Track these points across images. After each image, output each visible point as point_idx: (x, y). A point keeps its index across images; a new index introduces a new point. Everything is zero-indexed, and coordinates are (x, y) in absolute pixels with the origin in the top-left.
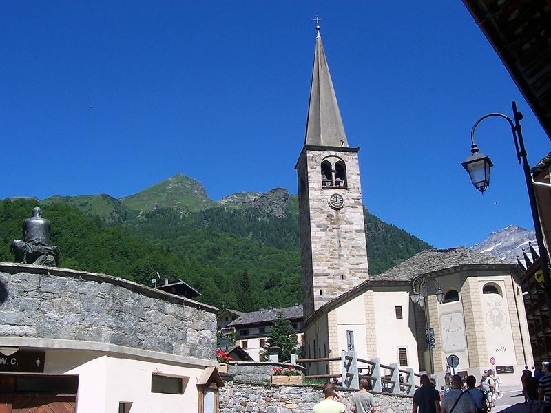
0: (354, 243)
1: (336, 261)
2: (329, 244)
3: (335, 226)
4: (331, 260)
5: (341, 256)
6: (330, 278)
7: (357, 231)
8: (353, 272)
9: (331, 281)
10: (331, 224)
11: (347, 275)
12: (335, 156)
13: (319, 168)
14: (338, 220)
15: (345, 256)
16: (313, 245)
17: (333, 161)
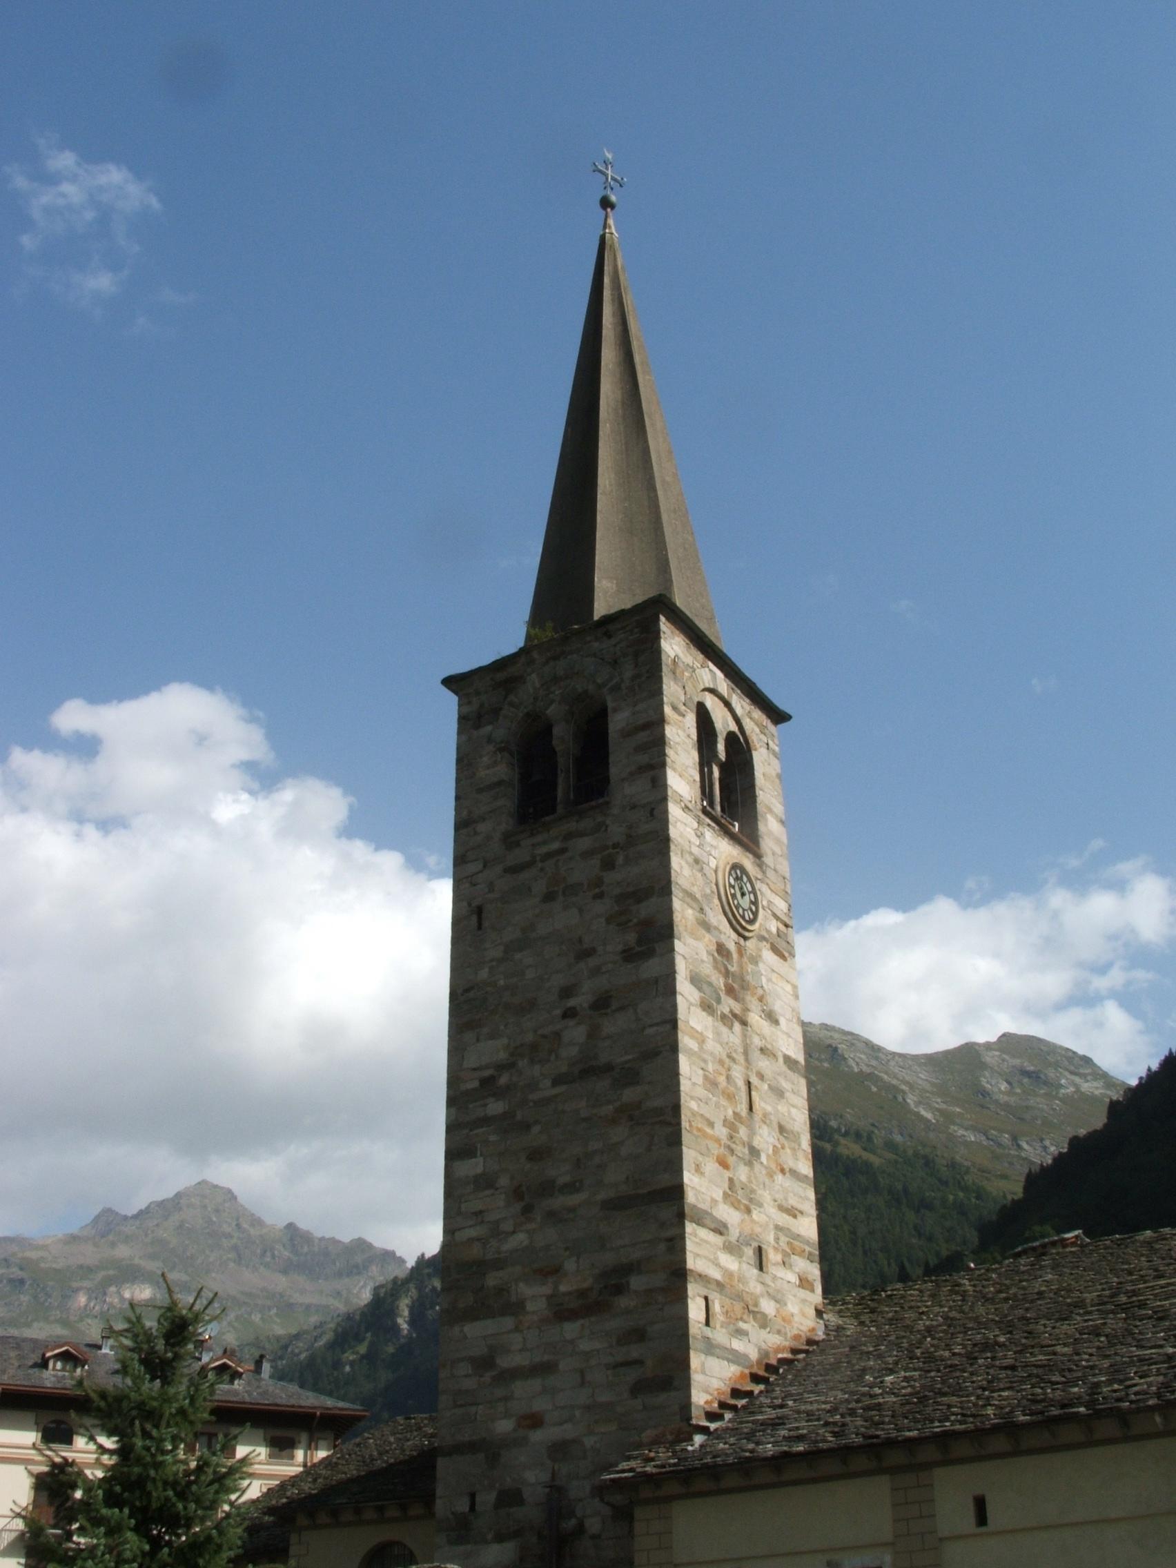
0: (782, 1108)
1: (742, 1173)
2: (722, 1080)
3: (737, 1008)
4: (731, 1160)
5: (754, 1152)
6: (730, 1248)
7: (789, 1061)
8: (783, 1240)
9: (730, 1262)
10: (730, 991)
11: (772, 1256)
12: (727, 704)
13: (691, 720)
14: (745, 986)
15: (764, 1159)
16: (685, 1065)
17: (723, 722)
